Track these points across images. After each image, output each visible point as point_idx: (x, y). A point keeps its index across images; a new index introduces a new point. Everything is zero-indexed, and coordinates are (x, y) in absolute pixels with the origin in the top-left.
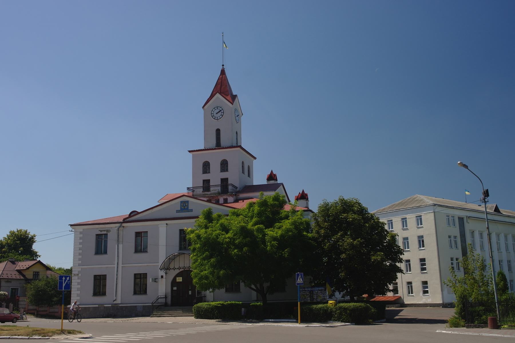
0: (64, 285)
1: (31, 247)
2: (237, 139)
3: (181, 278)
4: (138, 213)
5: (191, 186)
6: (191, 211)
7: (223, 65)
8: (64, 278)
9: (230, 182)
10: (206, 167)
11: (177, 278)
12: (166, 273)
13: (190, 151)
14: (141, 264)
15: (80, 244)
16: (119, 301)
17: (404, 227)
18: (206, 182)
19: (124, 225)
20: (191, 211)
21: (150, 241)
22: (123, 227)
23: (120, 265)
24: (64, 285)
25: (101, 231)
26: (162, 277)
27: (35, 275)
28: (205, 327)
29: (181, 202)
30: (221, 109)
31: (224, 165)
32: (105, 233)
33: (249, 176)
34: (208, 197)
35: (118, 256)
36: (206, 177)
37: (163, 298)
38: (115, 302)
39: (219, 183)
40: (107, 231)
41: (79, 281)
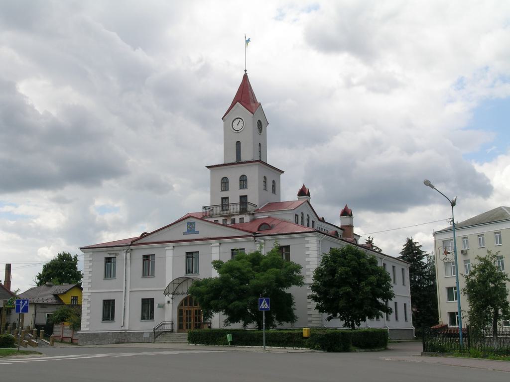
0: (21, 309)
1: (76, 268)
2: (260, 152)
4: (149, 234)
5: (208, 204)
6: (198, 232)
7: (246, 71)
8: (21, 302)
10: (225, 183)
12: (172, 298)
13: (208, 167)
15: (90, 267)
16: (127, 327)
17: (480, 245)
18: (225, 199)
19: (132, 247)
20: (198, 232)
22: (131, 250)
24: (21, 309)
26: (169, 302)
27: (73, 299)
28: (175, 352)
29: (188, 223)
31: (243, 181)
32: (114, 256)
33: (274, 191)
34: (224, 216)
35: (126, 280)
36: (225, 194)
37: (169, 324)
38: (123, 328)
39: (238, 201)
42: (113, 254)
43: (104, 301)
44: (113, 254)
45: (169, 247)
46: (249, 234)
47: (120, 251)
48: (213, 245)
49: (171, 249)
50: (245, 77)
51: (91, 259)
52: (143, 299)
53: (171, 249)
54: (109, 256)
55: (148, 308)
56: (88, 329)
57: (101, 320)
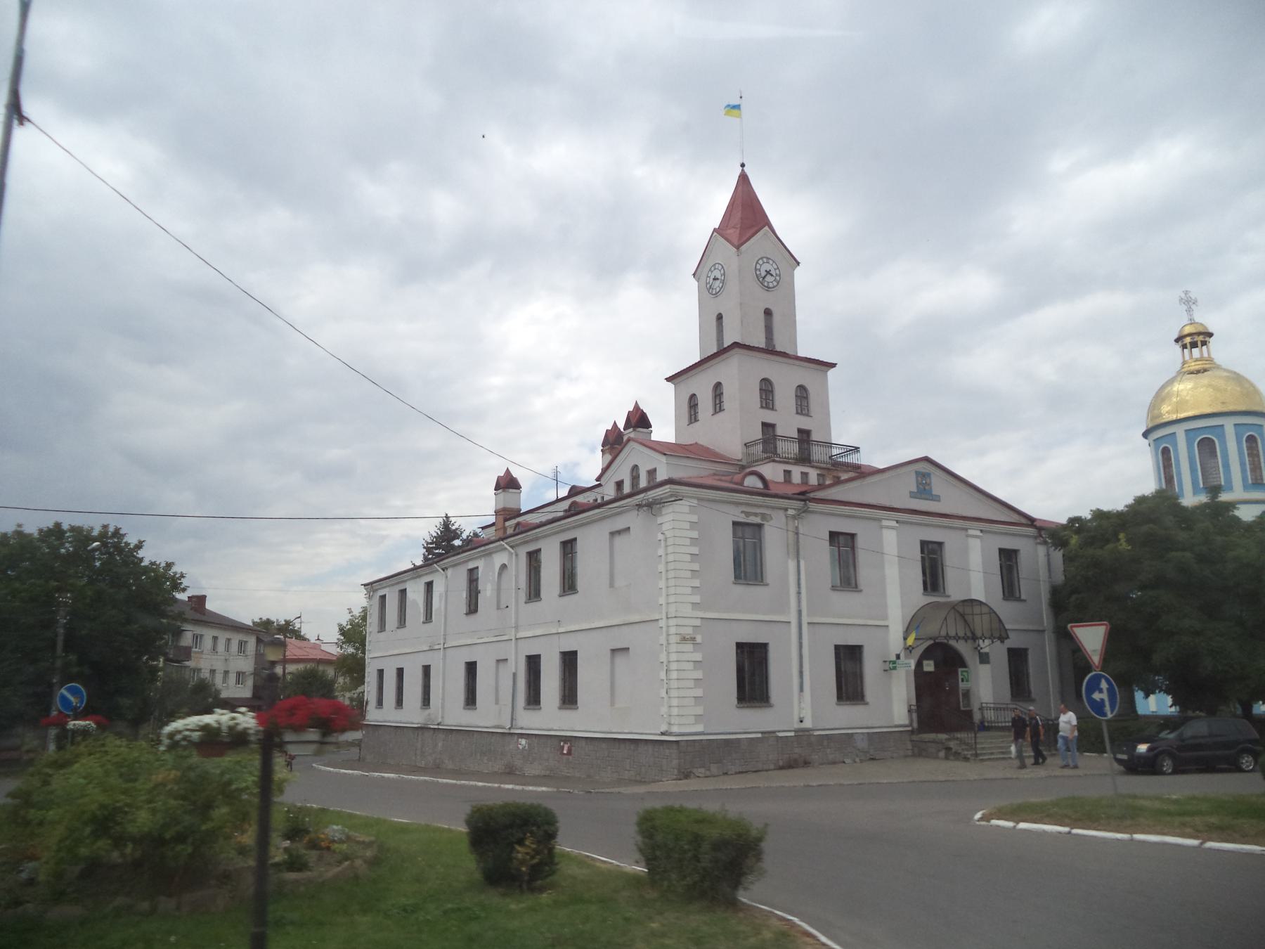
3: (932, 663)
6: (936, 498)
7: (743, 165)
9: (814, 437)
11: (925, 662)
16: (808, 724)
20: (936, 498)
23: (805, 620)
25: (748, 514)
32: (757, 520)
36: (769, 417)
40: (764, 516)
42: (756, 515)
43: (740, 646)
46: (1023, 521)
48: (971, 532)
49: (893, 528)
51: (694, 518)
53: (893, 528)
56: (700, 728)
57: (735, 701)
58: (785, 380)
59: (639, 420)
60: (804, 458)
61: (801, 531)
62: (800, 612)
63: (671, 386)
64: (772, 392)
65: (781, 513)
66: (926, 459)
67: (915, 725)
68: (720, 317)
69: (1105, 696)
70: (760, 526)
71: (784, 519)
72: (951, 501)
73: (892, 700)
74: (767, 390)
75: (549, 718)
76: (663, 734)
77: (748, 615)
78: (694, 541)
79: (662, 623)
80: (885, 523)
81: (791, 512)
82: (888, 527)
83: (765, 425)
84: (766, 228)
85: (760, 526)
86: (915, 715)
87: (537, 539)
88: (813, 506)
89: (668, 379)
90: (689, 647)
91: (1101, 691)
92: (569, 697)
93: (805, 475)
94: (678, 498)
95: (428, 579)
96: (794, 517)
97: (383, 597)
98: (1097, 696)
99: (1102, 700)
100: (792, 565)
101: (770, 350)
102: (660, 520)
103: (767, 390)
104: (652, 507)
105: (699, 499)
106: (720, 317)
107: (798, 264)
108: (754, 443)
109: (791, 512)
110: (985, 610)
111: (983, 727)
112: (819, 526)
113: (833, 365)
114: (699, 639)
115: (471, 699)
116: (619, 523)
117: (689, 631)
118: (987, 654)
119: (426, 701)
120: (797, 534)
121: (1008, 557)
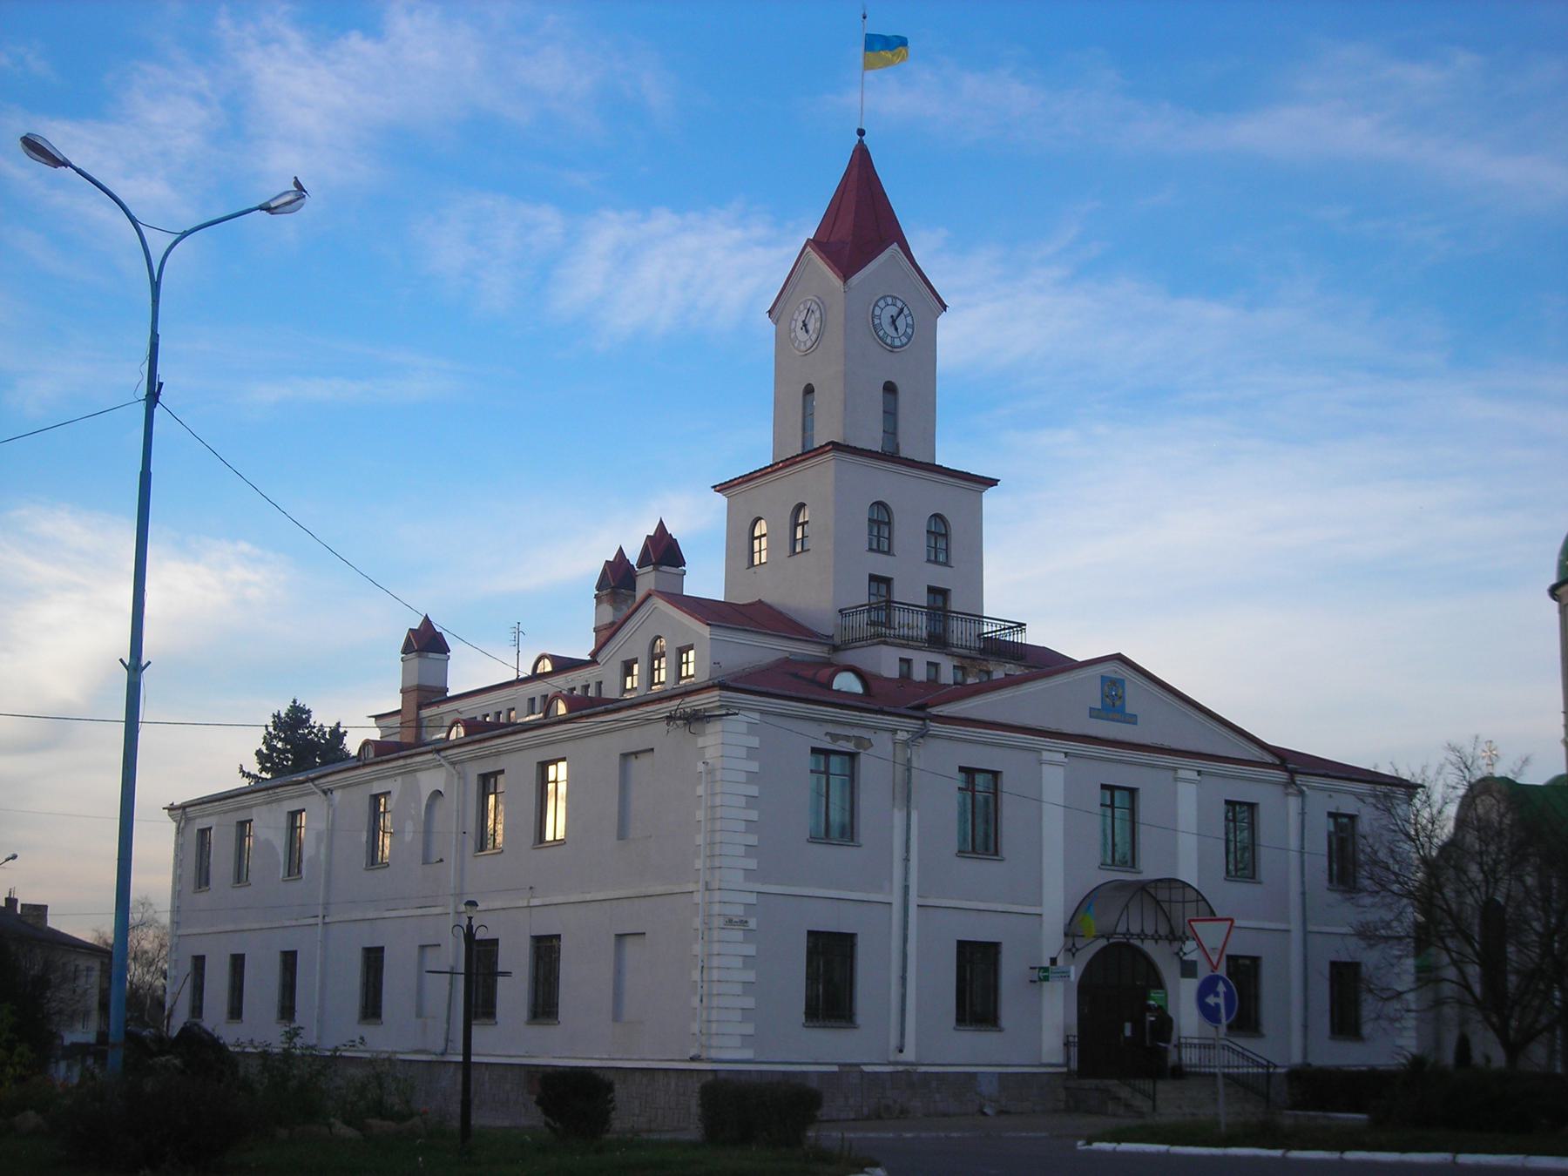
6: (1132, 720)
7: (861, 132)
9: (955, 604)
14: (977, 901)
16: (909, 1055)
20: (1132, 720)
21: (1011, 813)
25: (835, 737)
30: (900, 304)
32: (850, 747)
36: (881, 565)
40: (860, 741)
41: (750, 950)
42: (847, 738)
44: (847, 738)
45: (1053, 753)
46: (1268, 758)
47: (876, 729)
48: (1181, 774)
49: (1058, 764)
50: (861, 160)
51: (754, 742)
52: (959, 942)
53: (1058, 764)
54: (827, 744)
55: (977, 979)
56: (748, 1054)
58: (912, 502)
59: (664, 550)
60: (937, 641)
61: (915, 764)
62: (906, 888)
63: (721, 500)
64: (889, 524)
65: (887, 735)
66: (1119, 658)
67: (1074, 1065)
68: (809, 390)
69: (1221, 1001)
70: (852, 756)
71: (890, 746)
72: (1153, 726)
73: (1042, 1026)
74: (881, 519)
75: (510, 1040)
76: (692, 1059)
77: (830, 892)
78: (752, 777)
79: (698, 898)
80: (1046, 755)
81: (902, 736)
82: (1051, 763)
83: (873, 578)
84: (895, 246)
85: (852, 756)
86: (1074, 1051)
87: (498, 754)
88: (935, 728)
89: (721, 488)
90: (737, 935)
91: (1217, 995)
92: (544, 1006)
93: (933, 666)
94: (729, 712)
95: (295, 805)
96: (906, 743)
97: (204, 832)
98: (1211, 1000)
99: (1217, 1005)
100: (898, 817)
101: (890, 456)
102: (701, 742)
103: (881, 519)
104: (695, 719)
105: (762, 712)
106: (809, 390)
107: (945, 307)
108: (857, 610)
109: (902, 736)
110: (1191, 895)
111: (1178, 1073)
112: (942, 759)
113: (993, 482)
114: (752, 924)
115: (372, 1008)
116: (635, 739)
117: (737, 911)
118: (1194, 963)
119: (287, 1010)
120: (909, 770)
121: (1241, 814)
